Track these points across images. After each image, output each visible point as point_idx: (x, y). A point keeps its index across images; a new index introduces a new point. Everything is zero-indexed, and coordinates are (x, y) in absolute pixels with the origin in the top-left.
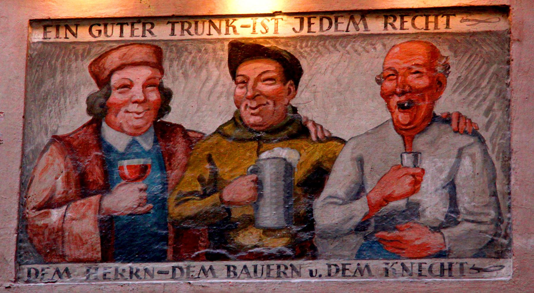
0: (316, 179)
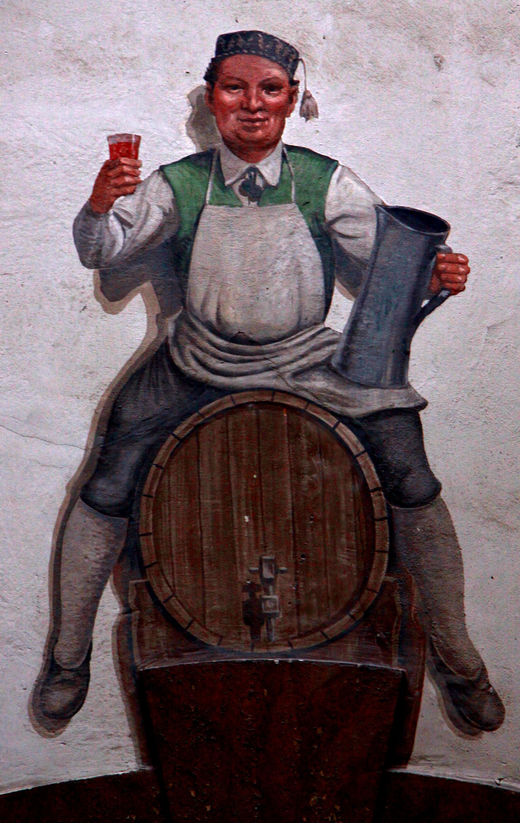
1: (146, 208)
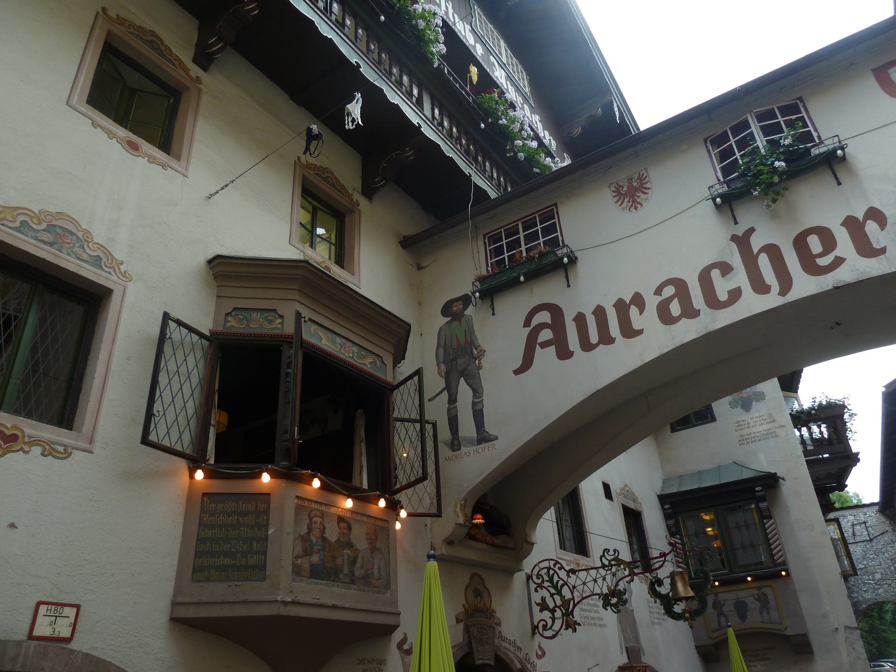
0: (354, 562)
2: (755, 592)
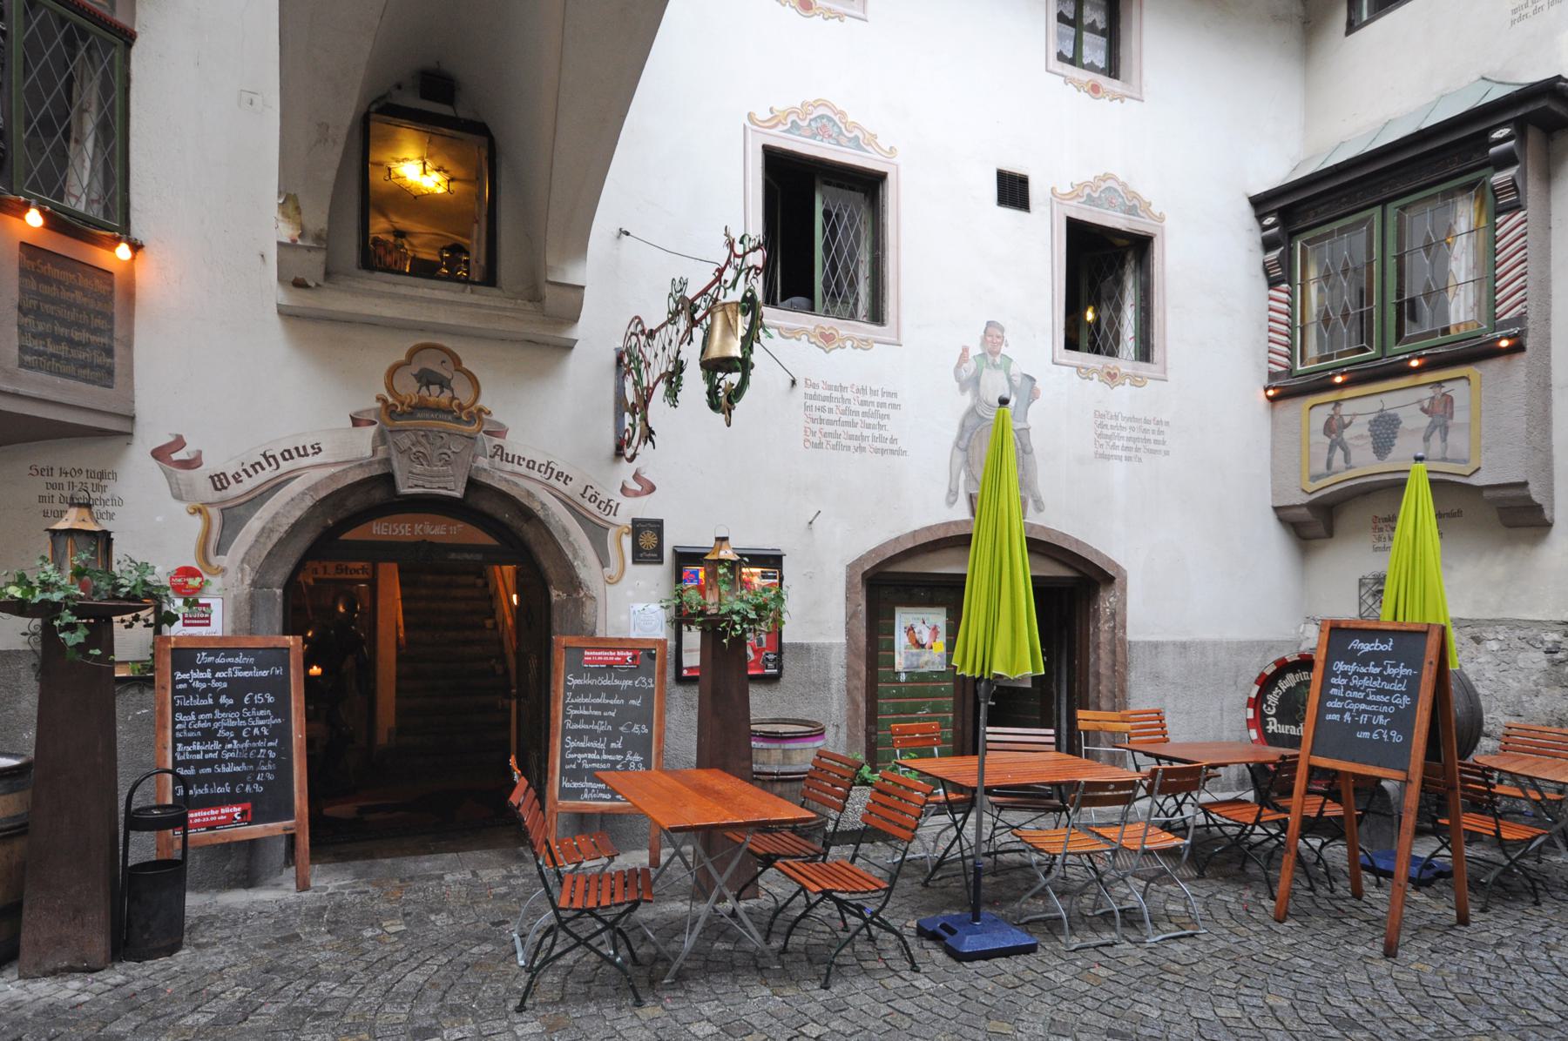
1: (970, 367)
2: (1427, 393)
